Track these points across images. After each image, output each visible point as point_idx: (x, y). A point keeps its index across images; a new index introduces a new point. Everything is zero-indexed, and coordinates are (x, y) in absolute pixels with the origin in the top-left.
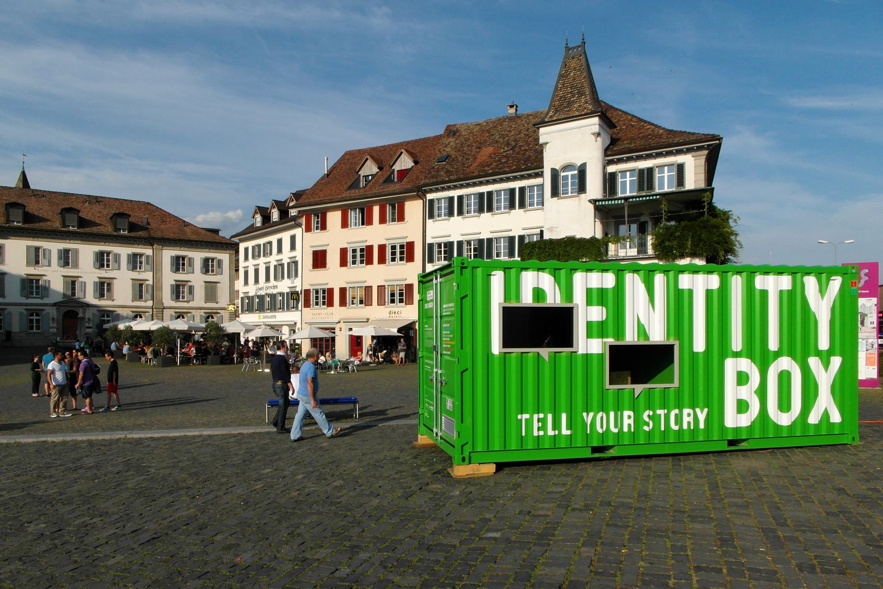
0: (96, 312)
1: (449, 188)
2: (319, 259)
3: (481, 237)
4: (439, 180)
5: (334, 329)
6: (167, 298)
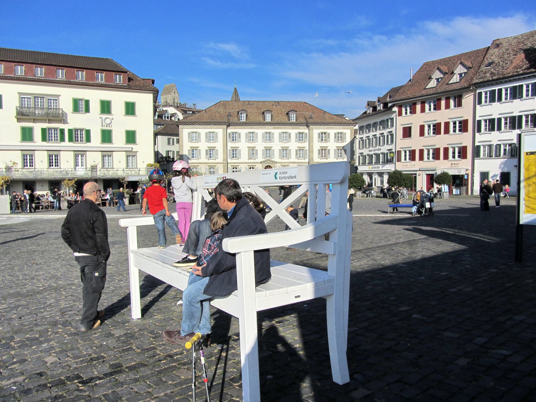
1: (492, 85)
2: (407, 132)
3: (514, 115)
4: (486, 80)
5: (416, 174)
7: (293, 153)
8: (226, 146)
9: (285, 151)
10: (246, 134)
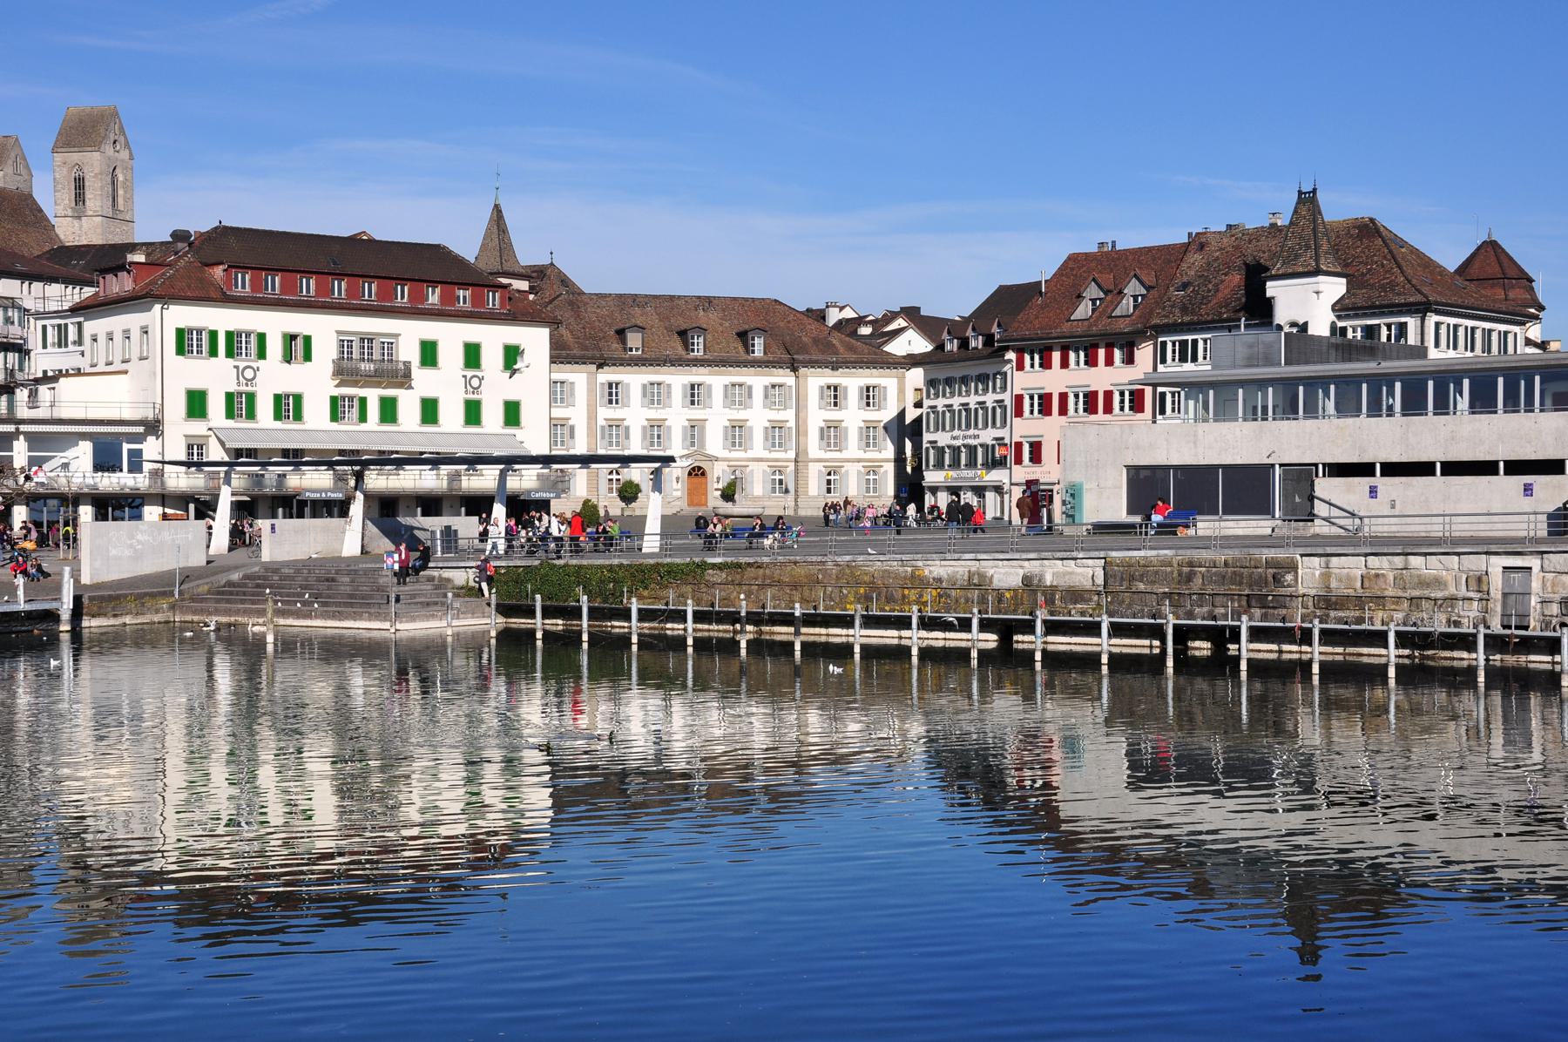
6: (814, 448)
8: (592, 416)
9: (737, 433)
10: (644, 386)
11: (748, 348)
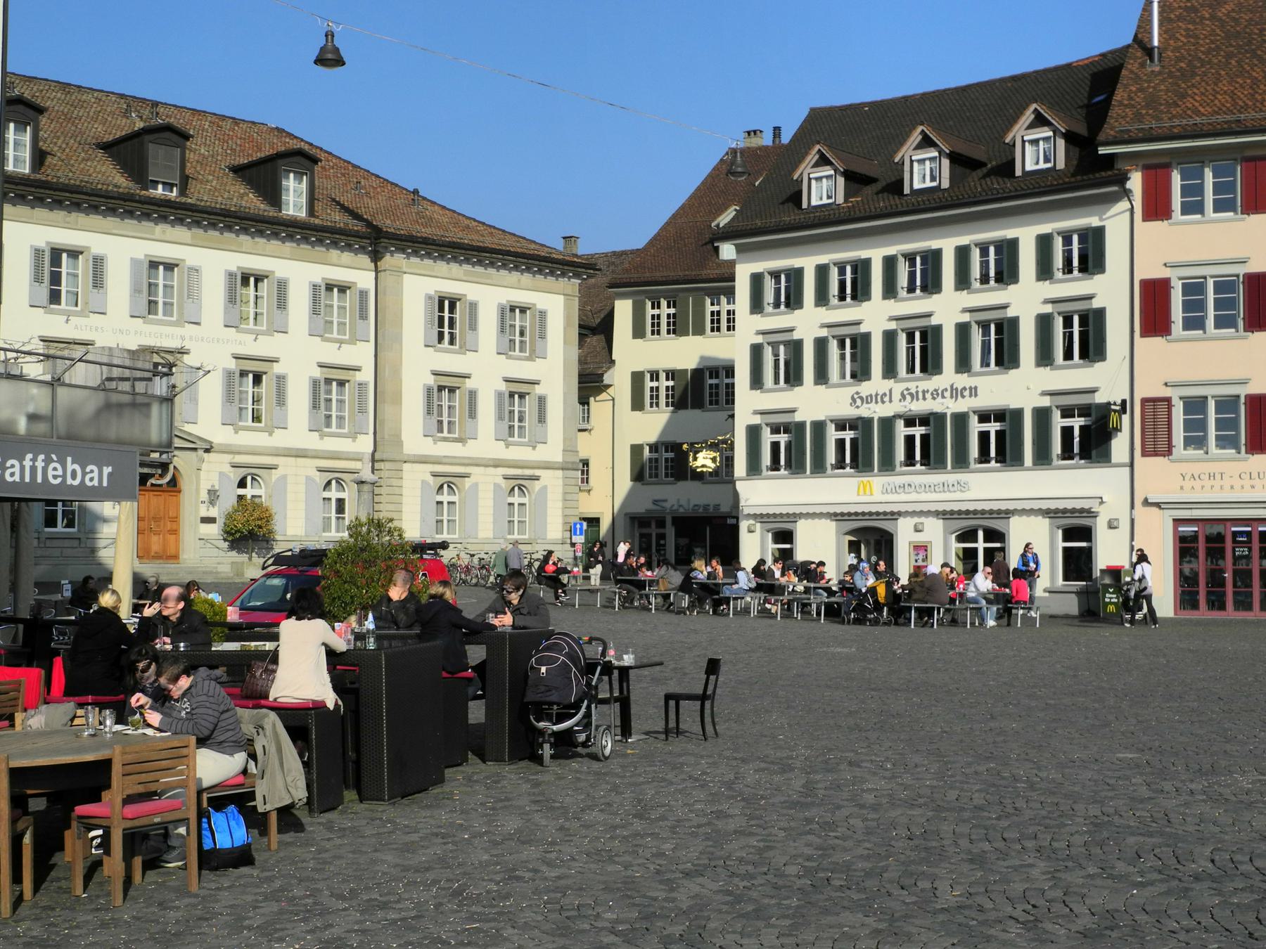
0: (227, 469)
7: (299, 396)
11: (273, 195)
